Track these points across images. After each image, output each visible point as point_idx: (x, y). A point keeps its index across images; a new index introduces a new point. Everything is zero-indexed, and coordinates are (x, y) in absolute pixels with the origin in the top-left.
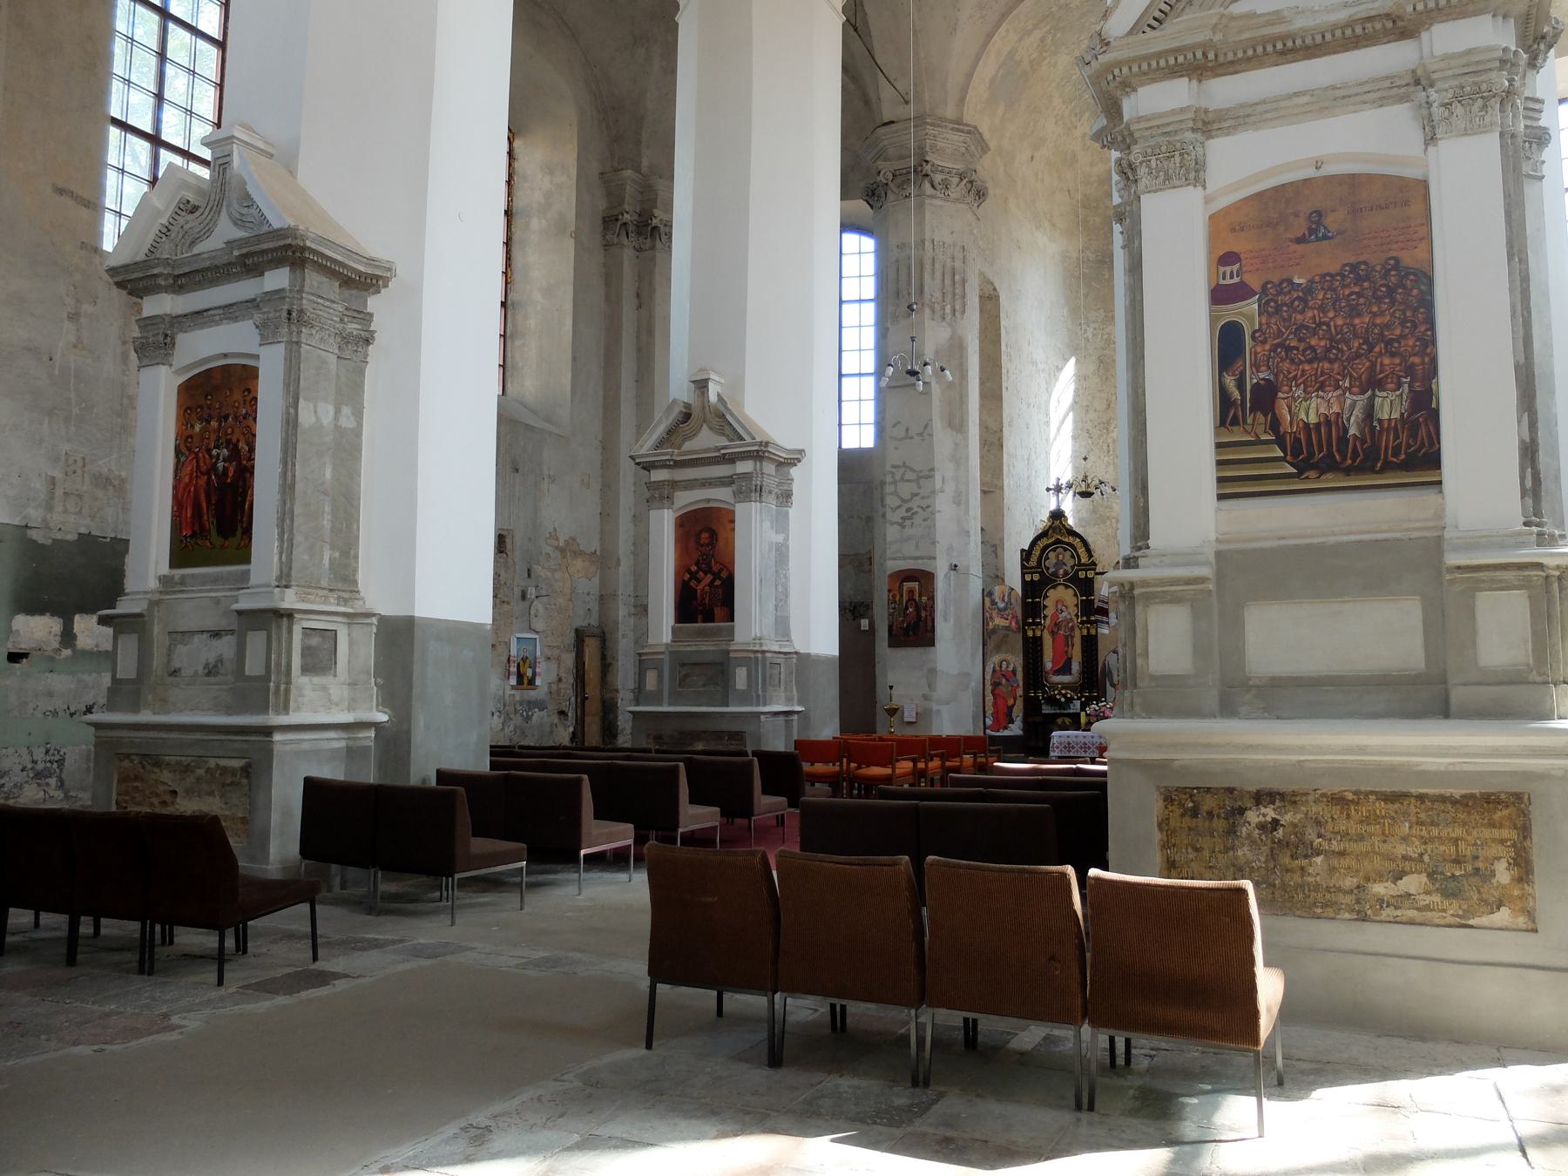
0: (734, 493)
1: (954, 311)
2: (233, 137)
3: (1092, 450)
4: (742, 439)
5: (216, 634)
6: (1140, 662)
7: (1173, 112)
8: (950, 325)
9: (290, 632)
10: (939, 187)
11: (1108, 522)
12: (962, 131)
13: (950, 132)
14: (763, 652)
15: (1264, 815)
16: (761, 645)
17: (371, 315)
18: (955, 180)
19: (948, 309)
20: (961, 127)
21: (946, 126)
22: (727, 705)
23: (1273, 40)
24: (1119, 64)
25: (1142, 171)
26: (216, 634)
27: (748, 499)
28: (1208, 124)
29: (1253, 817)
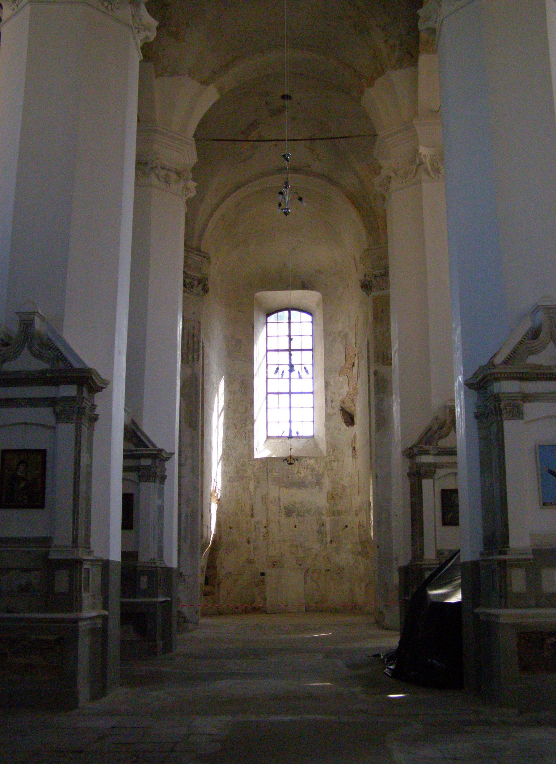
0: (139, 476)
1: (193, 358)
2: (38, 312)
3: (237, 436)
4: (148, 447)
5: (27, 570)
6: (509, 588)
7: (515, 393)
8: (191, 366)
9: (81, 570)
10: (188, 286)
11: (245, 480)
12: (200, 255)
13: (195, 255)
14: (157, 567)
15: (552, 641)
16: (155, 563)
17: (96, 406)
18: (196, 283)
19: (190, 358)
20: (201, 254)
21: (194, 253)
22: (135, 597)
23: (547, 374)
24: (498, 373)
25: (504, 412)
26: (27, 570)
27: (148, 480)
28: (526, 398)
29: (548, 641)
